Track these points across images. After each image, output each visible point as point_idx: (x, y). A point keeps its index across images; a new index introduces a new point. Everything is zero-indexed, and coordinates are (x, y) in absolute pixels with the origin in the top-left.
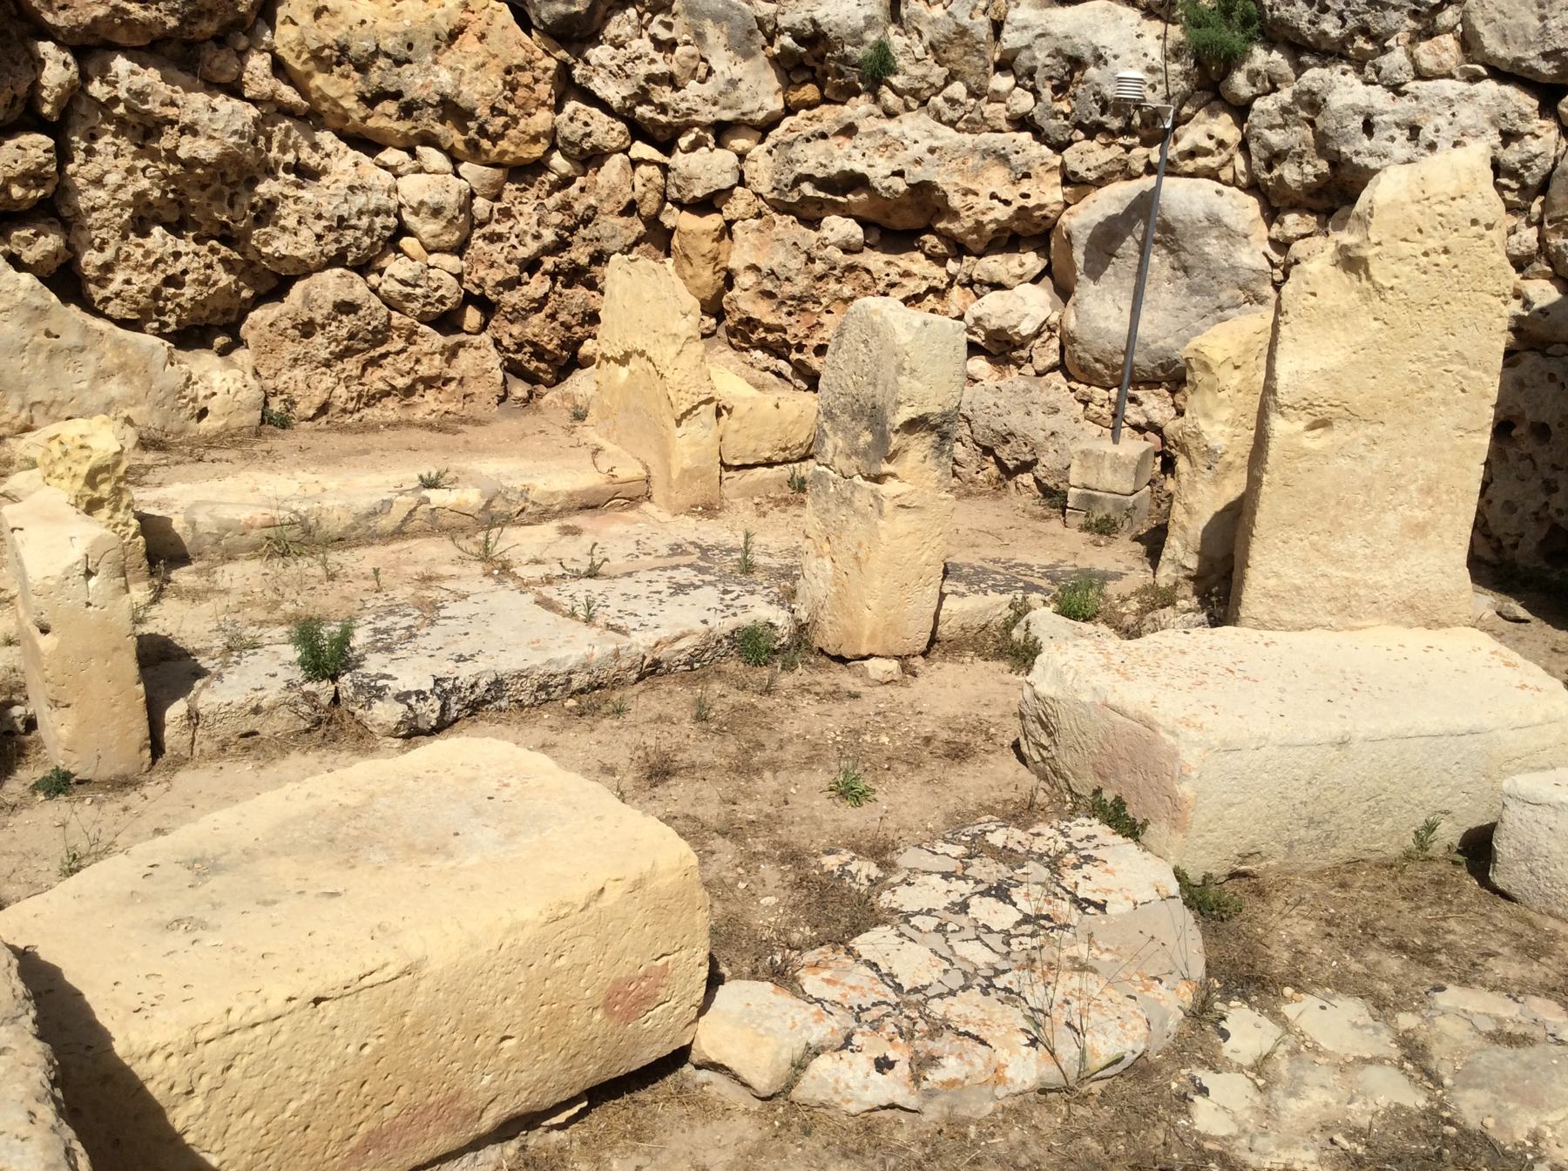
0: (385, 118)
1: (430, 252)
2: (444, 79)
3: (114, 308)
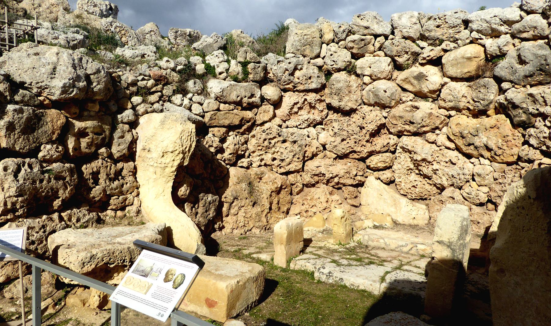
0: (470, 150)
1: (479, 186)
2: (484, 140)
3: (402, 192)
